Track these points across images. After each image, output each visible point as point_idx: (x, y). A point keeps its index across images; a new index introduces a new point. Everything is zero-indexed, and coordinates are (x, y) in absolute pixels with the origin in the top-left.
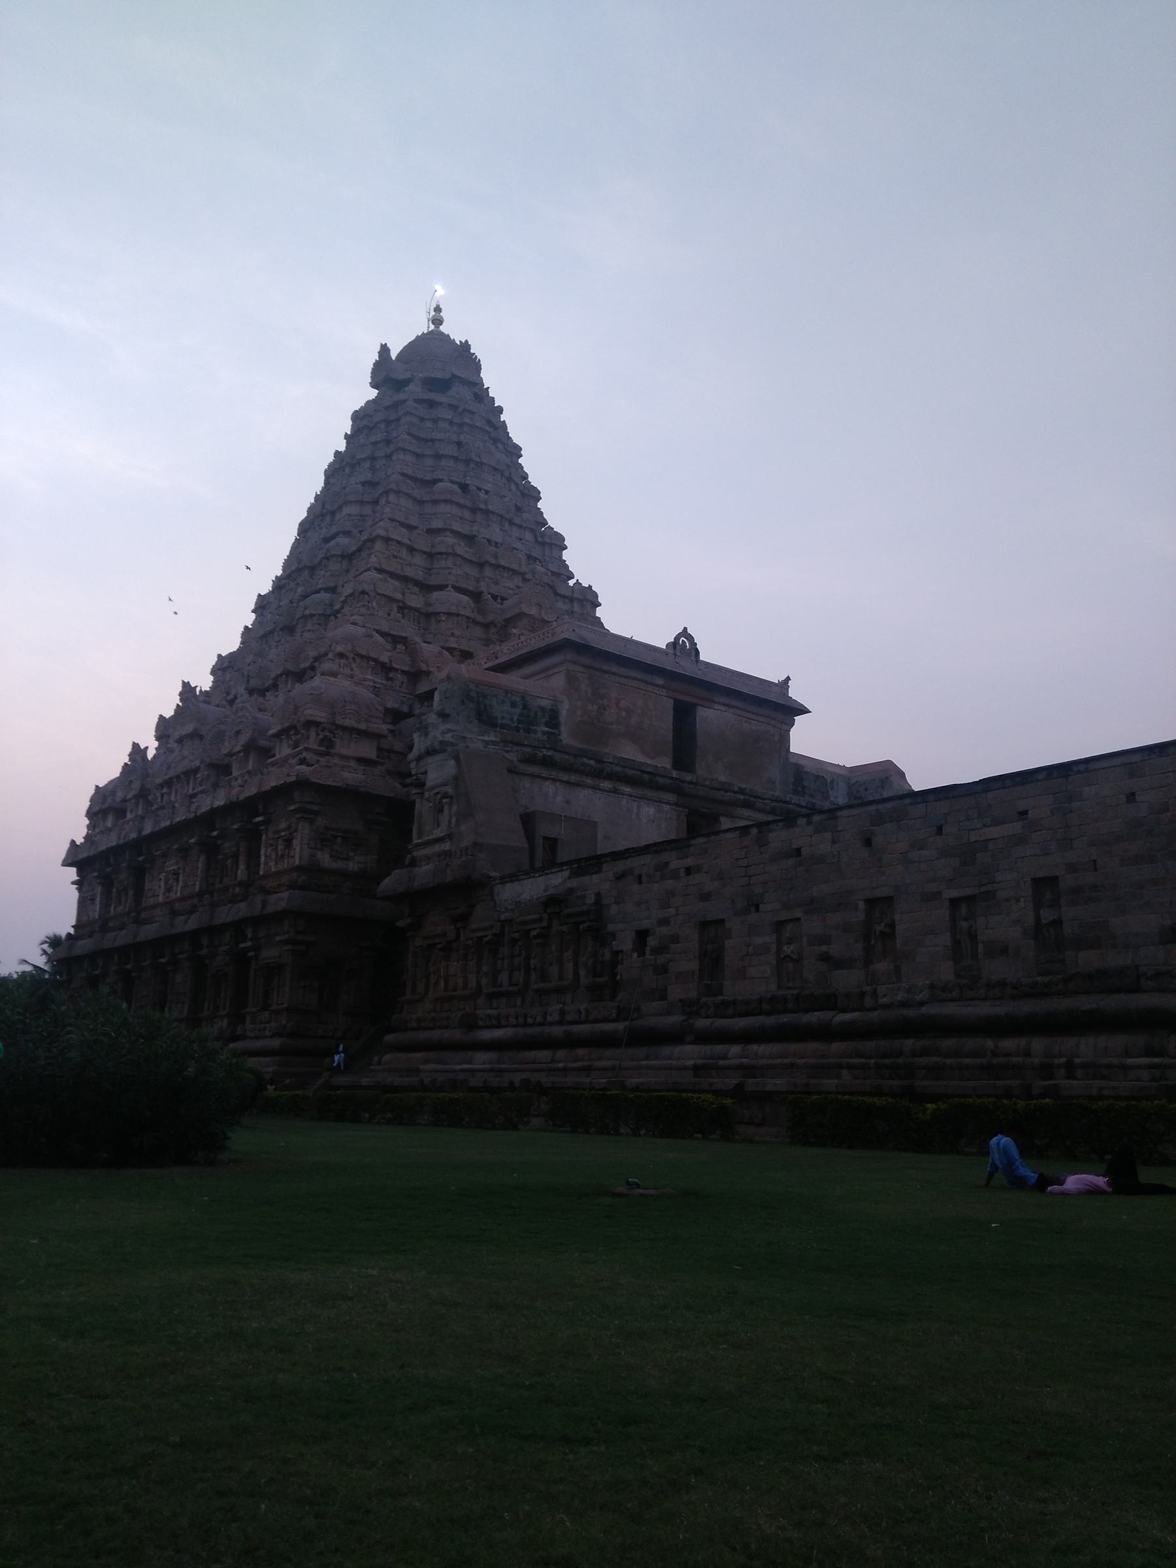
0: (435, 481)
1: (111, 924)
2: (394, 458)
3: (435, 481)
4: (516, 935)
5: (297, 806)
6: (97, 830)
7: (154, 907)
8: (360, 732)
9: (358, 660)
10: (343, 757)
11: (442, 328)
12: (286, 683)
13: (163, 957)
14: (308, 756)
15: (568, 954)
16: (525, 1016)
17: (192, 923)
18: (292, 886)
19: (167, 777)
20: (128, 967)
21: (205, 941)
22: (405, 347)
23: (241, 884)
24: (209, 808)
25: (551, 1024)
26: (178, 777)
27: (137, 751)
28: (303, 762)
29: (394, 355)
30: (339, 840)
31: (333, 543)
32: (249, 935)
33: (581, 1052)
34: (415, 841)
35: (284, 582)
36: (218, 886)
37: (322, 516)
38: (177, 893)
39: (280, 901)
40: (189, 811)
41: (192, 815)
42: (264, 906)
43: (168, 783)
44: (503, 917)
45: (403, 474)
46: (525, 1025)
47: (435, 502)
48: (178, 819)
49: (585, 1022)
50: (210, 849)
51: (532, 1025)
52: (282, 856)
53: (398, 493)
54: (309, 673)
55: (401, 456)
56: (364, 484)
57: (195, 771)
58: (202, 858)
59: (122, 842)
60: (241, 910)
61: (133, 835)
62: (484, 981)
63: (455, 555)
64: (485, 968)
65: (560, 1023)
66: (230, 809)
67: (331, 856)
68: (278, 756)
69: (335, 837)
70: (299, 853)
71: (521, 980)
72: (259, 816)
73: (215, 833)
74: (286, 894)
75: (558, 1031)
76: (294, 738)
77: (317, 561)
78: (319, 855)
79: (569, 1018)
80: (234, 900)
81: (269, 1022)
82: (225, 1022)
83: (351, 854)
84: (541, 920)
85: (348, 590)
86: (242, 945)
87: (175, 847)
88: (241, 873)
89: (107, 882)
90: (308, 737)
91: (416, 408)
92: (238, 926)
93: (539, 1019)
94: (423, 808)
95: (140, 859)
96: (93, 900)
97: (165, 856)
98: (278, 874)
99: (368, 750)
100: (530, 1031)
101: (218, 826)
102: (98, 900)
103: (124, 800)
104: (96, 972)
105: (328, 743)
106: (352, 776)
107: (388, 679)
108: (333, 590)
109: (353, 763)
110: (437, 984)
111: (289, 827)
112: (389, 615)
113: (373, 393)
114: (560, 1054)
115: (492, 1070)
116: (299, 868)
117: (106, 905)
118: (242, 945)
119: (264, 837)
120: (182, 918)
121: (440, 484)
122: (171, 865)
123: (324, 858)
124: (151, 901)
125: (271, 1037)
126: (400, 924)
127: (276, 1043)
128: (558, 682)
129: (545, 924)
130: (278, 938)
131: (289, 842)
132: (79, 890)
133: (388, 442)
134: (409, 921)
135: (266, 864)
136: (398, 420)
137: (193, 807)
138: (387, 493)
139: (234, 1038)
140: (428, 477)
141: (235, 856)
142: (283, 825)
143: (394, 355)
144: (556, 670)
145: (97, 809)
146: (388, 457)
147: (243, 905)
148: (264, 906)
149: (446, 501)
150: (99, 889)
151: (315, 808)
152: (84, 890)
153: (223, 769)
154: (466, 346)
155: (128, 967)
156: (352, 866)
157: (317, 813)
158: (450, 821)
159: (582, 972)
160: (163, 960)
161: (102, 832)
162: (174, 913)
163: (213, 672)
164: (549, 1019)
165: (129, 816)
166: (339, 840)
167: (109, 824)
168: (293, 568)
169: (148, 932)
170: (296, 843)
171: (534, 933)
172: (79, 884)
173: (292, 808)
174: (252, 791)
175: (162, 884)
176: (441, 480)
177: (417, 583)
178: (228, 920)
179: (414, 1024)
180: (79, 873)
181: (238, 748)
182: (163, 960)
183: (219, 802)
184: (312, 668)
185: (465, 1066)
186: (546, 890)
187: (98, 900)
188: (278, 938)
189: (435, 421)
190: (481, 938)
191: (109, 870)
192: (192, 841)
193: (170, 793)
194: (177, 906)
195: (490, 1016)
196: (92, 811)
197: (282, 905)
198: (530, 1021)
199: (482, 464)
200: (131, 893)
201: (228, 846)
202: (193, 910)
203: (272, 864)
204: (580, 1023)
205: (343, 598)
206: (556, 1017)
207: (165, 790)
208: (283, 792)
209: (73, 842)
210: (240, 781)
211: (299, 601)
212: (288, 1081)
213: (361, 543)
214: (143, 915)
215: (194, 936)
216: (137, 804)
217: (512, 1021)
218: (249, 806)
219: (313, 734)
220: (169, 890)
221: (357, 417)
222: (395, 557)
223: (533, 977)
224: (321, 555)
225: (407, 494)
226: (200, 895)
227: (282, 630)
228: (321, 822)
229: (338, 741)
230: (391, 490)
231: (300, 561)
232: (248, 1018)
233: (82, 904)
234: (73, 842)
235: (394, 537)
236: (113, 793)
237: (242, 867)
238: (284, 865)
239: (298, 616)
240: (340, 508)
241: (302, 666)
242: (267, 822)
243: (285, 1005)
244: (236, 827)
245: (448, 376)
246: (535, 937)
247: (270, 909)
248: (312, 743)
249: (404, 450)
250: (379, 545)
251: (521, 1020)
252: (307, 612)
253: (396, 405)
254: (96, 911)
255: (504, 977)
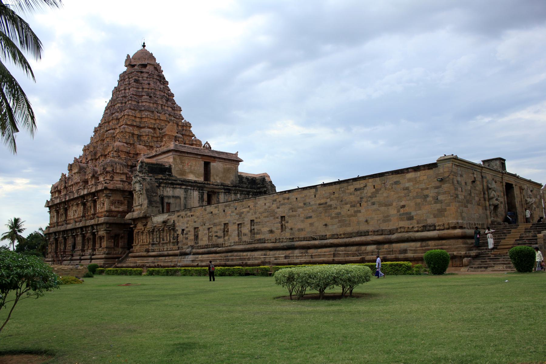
0: (142, 96)
1: (59, 224)
2: (131, 89)
3: (142, 96)
4: (157, 230)
5: (105, 195)
6: (54, 197)
7: (70, 219)
8: (121, 173)
9: (120, 152)
10: (116, 181)
11: (145, 48)
12: (102, 158)
13: (74, 233)
14: (108, 181)
15: (168, 235)
16: (159, 249)
17: (80, 225)
18: (105, 216)
19: (72, 184)
20: (65, 236)
21: (84, 229)
22: (134, 54)
23: (92, 214)
24: (83, 194)
25: (165, 251)
26: (74, 184)
27: (64, 175)
28: (106, 183)
29: (131, 58)
30: (117, 203)
31: (114, 115)
32: (95, 228)
33: (171, 257)
34: (134, 205)
35: (101, 125)
36: (87, 215)
37: (111, 106)
38: (76, 216)
39: (102, 220)
40: (78, 194)
41: (79, 196)
42: (98, 221)
43: (72, 185)
44: (154, 225)
45: (133, 94)
46: (160, 251)
47: (142, 102)
48: (75, 196)
49: (172, 250)
50: (84, 204)
51: (161, 251)
52: (102, 208)
53: (131, 100)
54: (108, 155)
55: (132, 89)
56: (122, 97)
57: (79, 183)
58: (82, 207)
59: (61, 201)
60: (93, 222)
61: (64, 200)
62: (151, 241)
63: (148, 118)
64: (151, 238)
65: (167, 251)
66: (87, 195)
67: (115, 207)
68: (100, 181)
69: (116, 202)
70: (106, 207)
71: (159, 241)
72: (95, 196)
73: (85, 201)
74: (103, 218)
75: (166, 253)
76: (104, 176)
77: (110, 120)
78: (112, 207)
79: (168, 250)
80: (91, 219)
81: (101, 251)
82: (91, 250)
83: (120, 206)
84: (162, 226)
85: (118, 131)
86: (94, 231)
87: (75, 204)
88: (92, 212)
89: (58, 212)
90: (107, 176)
91: (137, 74)
92: (92, 226)
93: (162, 250)
94: (135, 196)
95: (66, 206)
96: (54, 217)
97: (72, 206)
98: (101, 212)
99: (124, 177)
100: (160, 253)
101: (86, 198)
102: (55, 217)
103: (61, 189)
104: (57, 237)
105: (112, 177)
106: (120, 186)
107: (129, 156)
108: (114, 129)
109: (119, 182)
110: (140, 241)
111: (103, 200)
112: (129, 137)
113: (125, 69)
114: (167, 258)
115: (152, 262)
116: (107, 211)
117: (58, 218)
118: (94, 231)
119: (97, 202)
120: (78, 223)
121: (144, 97)
122: (74, 208)
123: (113, 208)
124: (70, 218)
125: (103, 254)
126: (131, 226)
127: (103, 256)
128: (171, 160)
129: (163, 227)
130: (102, 229)
131: (104, 204)
132: (50, 214)
133: (129, 84)
134: (133, 226)
135: (98, 209)
136: (132, 78)
137: (79, 193)
138: (128, 101)
139: (93, 255)
140: (140, 94)
141: (91, 207)
142: (102, 199)
143: (131, 58)
144: (171, 157)
145: (53, 191)
146: (129, 89)
147: (93, 220)
148: (98, 221)
149: (145, 102)
150: (55, 214)
151: (110, 195)
152: (51, 213)
153: (86, 182)
154: (152, 54)
155: (65, 236)
156: (121, 209)
157: (110, 196)
158: (142, 200)
159: (171, 239)
160: (74, 234)
161: (55, 198)
162: (76, 222)
163: (83, 150)
164: (164, 250)
165: (62, 194)
166: (117, 203)
167: (57, 195)
168: (104, 122)
169: (69, 227)
170: (105, 204)
171: (160, 229)
172: (50, 212)
173: (104, 195)
174: (93, 190)
175: (72, 213)
176: (144, 95)
177: (138, 127)
178: (89, 224)
179: (136, 251)
180: (50, 209)
181: (90, 177)
182: (74, 234)
183: (85, 193)
184: (108, 154)
185: (147, 261)
186: (163, 219)
187: (55, 217)
188: (102, 229)
189: (143, 77)
190: (149, 230)
191: (58, 209)
192: (79, 202)
193: (72, 188)
194: (77, 220)
195: (152, 249)
196: (52, 192)
197: (102, 221)
198: (160, 250)
199: (156, 89)
200: (64, 215)
201: (89, 204)
202: (81, 221)
203: (100, 209)
204: (170, 251)
205: (116, 133)
206: (166, 249)
207: (71, 187)
208: (101, 191)
209: (47, 201)
210: (91, 186)
211: (105, 132)
212: (107, 265)
213: (121, 116)
214: (68, 222)
215: (81, 228)
216: (64, 190)
217: (157, 250)
218: (93, 194)
219: (108, 175)
220: (74, 215)
221: (120, 76)
222: (131, 120)
223: (161, 240)
224: (111, 119)
225: (135, 101)
226: (82, 217)
227: (101, 141)
228: (111, 198)
229: (115, 177)
230: (130, 100)
231: (105, 120)
232: (96, 250)
233: (51, 218)
234: (47, 201)
235: (130, 114)
236: (57, 187)
237: (92, 210)
238: (103, 210)
239: (105, 137)
240: (116, 104)
241: (106, 153)
242: (98, 198)
243: (105, 246)
244: (90, 199)
245: (146, 63)
246: (161, 230)
247: (99, 222)
248: (108, 178)
249: (133, 87)
250: (126, 117)
251: (159, 250)
252: (107, 136)
253: (131, 73)
254: (55, 220)
255: (155, 240)
